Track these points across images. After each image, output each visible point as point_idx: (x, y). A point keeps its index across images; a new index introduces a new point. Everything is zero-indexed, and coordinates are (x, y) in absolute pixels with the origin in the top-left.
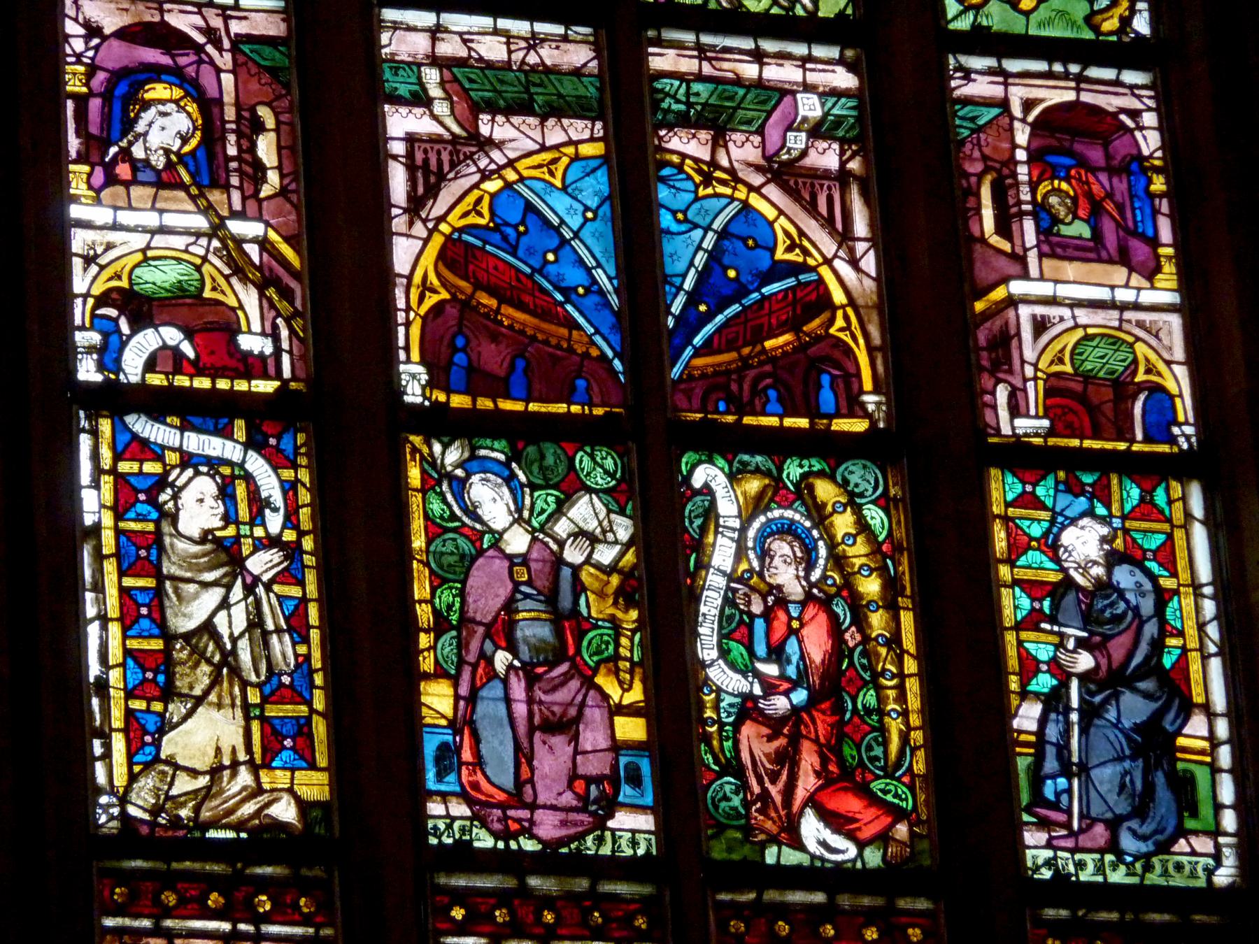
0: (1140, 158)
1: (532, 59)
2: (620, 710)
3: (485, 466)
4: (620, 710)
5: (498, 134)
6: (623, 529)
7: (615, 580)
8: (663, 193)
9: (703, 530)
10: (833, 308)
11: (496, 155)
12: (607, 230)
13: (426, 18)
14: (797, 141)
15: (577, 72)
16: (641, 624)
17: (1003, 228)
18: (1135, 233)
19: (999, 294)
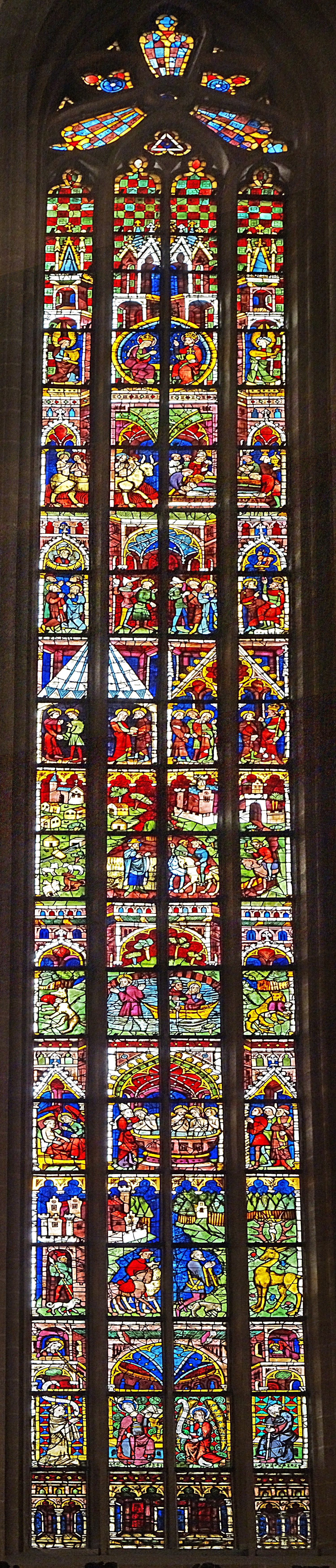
0: (297, 1338)
1: (145, 1329)
2: (157, 1442)
3: (127, 1401)
4: (157, 1442)
5: (135, 1343)
6: (160, 1411)
7: (157, 1420)
8: (175, 1351)
9: (180, 1411)
10: (216, 1370)
11: (135, 1347)
12: (161, 1359)
13: (120, 1323)
14: (209, 1340)
15: (156, 1331)
16: (163, 1427)
17: (260, 1353)
18: (294, 1352)
19: (258, 1365)
